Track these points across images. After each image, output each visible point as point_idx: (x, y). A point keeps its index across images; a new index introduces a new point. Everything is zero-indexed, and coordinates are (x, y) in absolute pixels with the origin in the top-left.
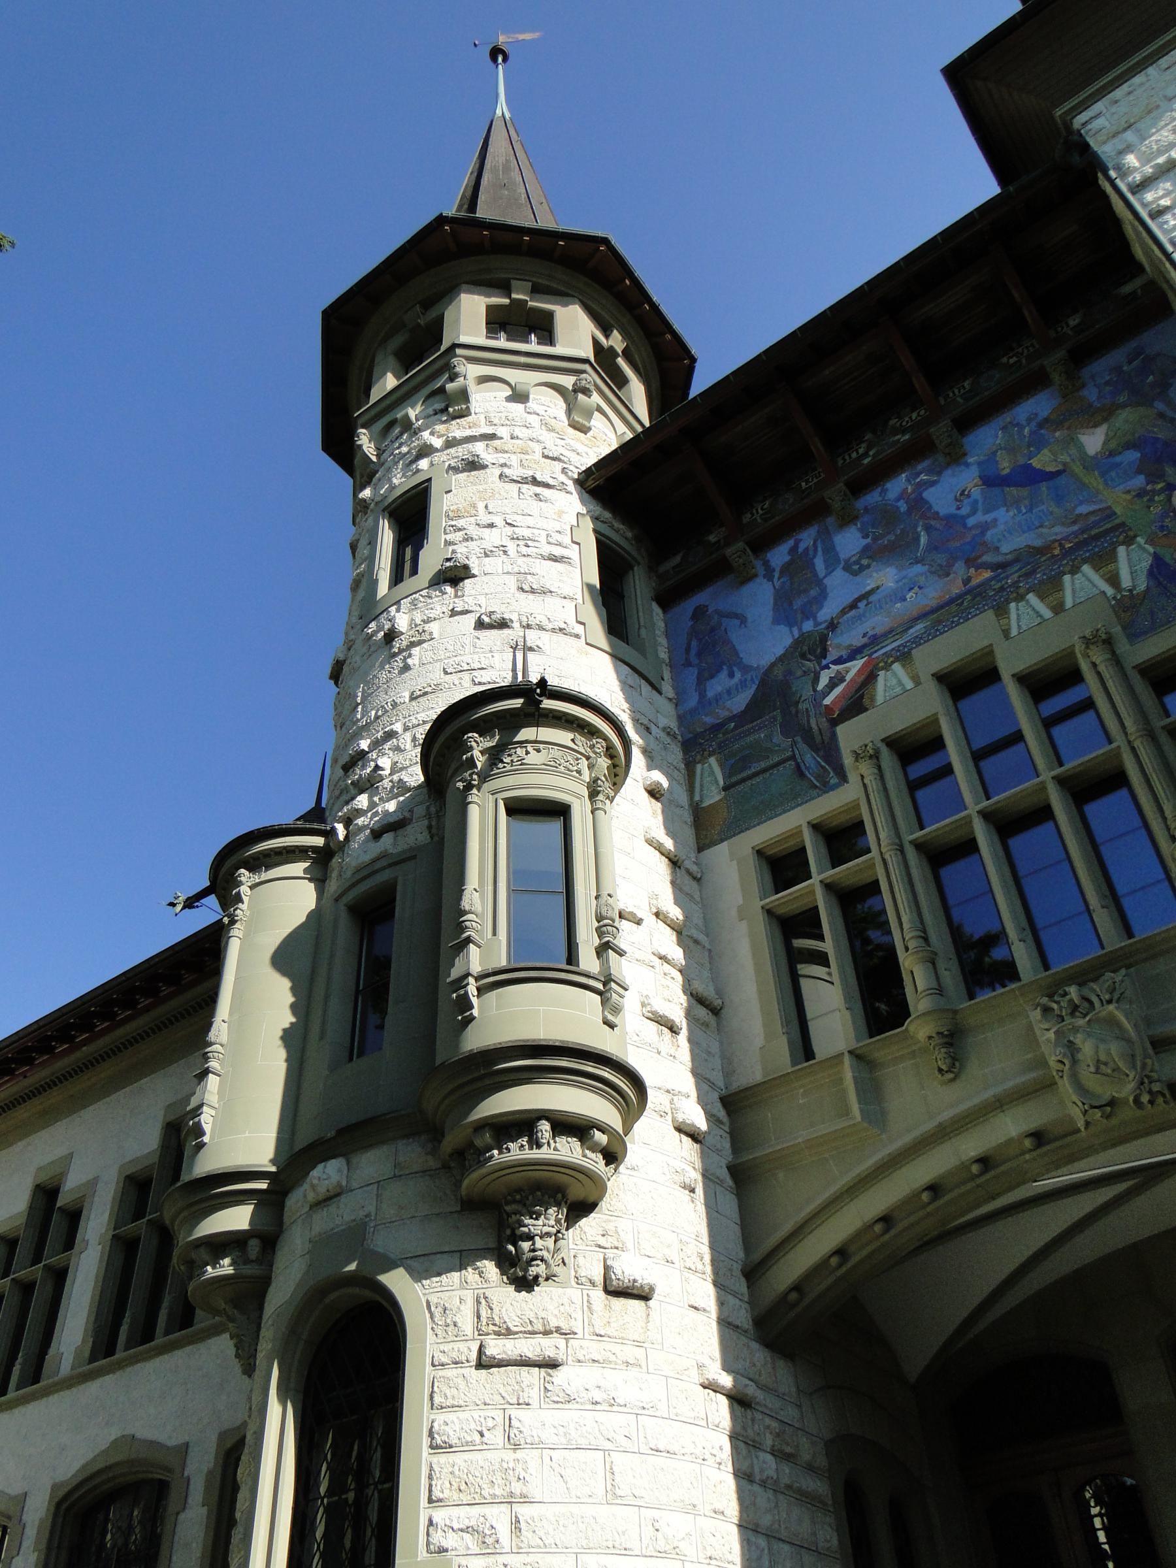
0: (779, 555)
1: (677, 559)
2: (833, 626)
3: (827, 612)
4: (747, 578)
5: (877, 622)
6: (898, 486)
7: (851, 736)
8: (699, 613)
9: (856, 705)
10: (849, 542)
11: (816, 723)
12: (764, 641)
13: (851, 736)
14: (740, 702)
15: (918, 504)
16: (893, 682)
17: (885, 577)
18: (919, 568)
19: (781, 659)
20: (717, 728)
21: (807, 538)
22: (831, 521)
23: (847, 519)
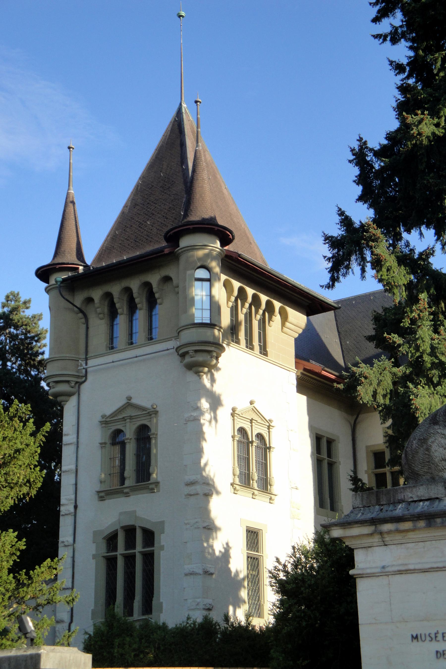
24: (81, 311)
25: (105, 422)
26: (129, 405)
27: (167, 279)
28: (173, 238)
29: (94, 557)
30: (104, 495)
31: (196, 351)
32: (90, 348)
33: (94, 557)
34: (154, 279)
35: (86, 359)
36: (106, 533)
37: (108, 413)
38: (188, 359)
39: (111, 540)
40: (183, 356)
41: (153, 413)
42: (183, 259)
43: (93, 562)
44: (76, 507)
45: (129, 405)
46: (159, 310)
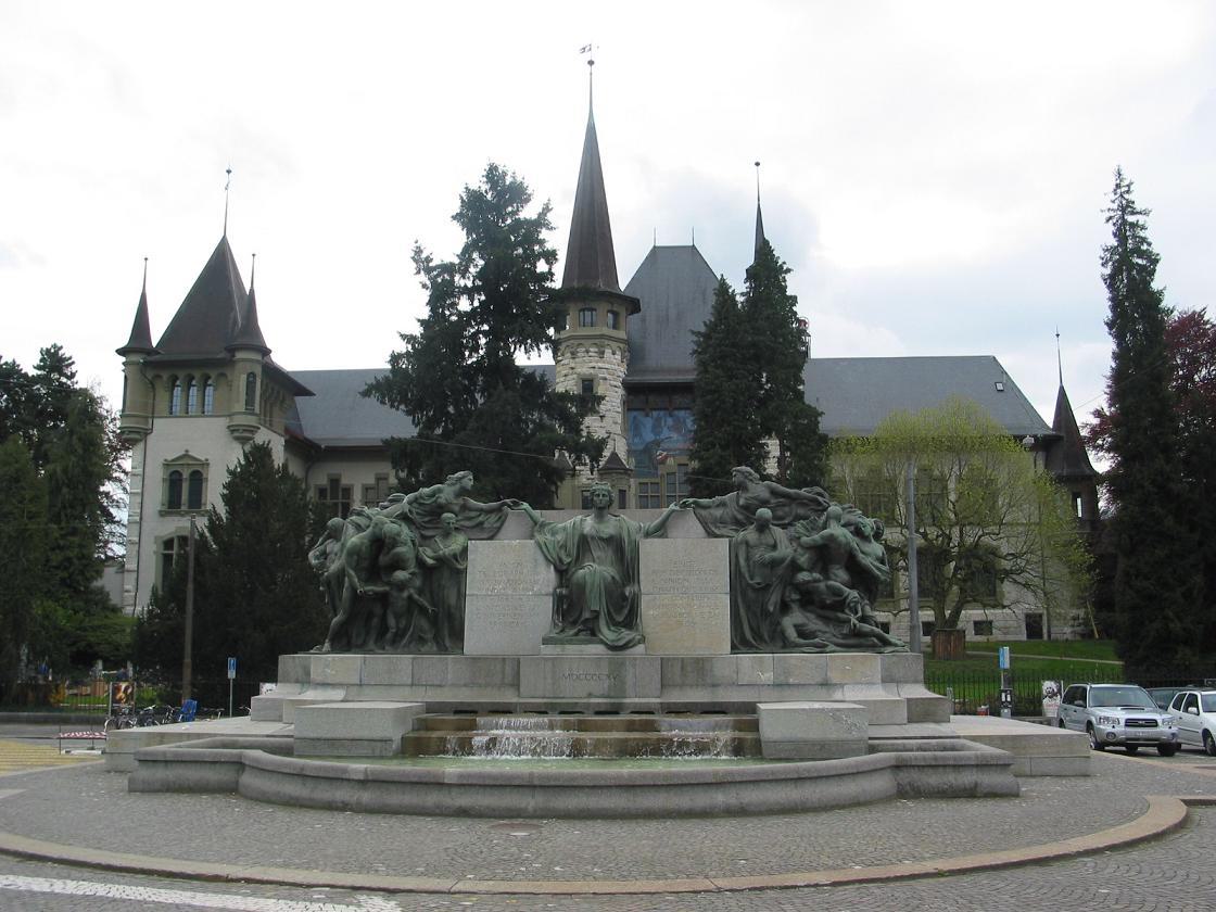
0: (655, 413)
1: (631, 397)
2: (663, 440)
3: (662, 437)
4: (647, 415)
5: (671, 446)
6: (682, 413)
7: (660, 467)
8: (635, 417)
9: (663, 462)
10: (670, 421)
11: (655, 462)
12: (649, 437)
13: (660, 467)
14: (641, 447)
15: (684, 421)
16: (670, 461)
17: (675, 436)
18: (680, 438)
19: (653, 442)
20: (635, 451)
21: (662, 413)
22: (667, 412)
23: (671, 416)
24: (151, 383)
25: (167, 465)
26: (186, 455)
27: (223, 375)
28: (232, 350)
29: (155, 552)
30: (162, 514)
31: (244, 430)
32: (156, 409)
33: (155, 552)
34: (213, 374)
35: (153, 417)
36: (165, 539)
37: (170, 458)
38: (236, 434)
39: (168, 544)
40: (232, 431)
41: (206, 464)
42: (240, 366)
43: (154, 557)
44: (141, 519)
45: (186, 455)
46: (210, 390)
